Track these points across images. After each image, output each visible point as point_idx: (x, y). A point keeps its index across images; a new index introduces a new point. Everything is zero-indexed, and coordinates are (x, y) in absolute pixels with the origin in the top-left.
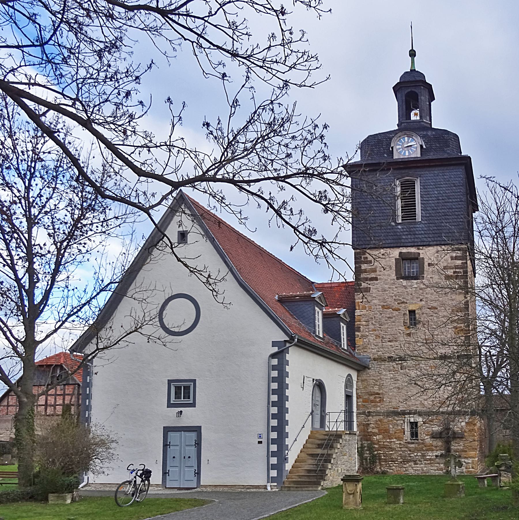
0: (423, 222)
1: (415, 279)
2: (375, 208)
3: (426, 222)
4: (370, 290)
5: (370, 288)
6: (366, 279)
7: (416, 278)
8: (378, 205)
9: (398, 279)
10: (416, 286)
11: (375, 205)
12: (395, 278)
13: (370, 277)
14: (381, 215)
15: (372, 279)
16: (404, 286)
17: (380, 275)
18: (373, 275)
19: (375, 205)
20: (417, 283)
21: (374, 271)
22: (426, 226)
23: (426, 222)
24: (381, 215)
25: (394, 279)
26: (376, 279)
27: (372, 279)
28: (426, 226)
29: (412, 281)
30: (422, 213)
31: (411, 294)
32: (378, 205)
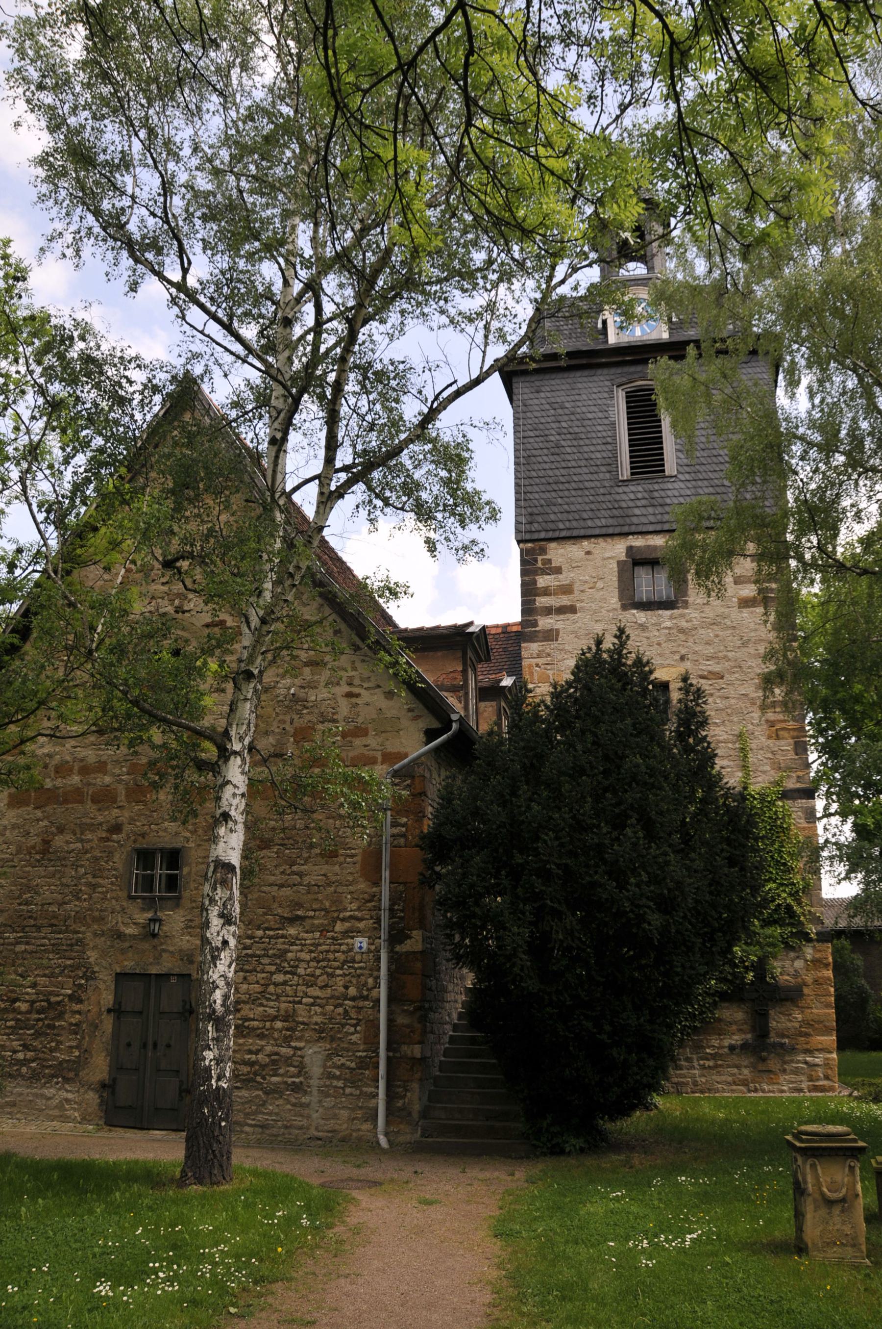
0: (680, 476)
1: (666, 609)
2: (568, 450)
3: (687, 477)
4: (558, 635)
5: (557, 631)
6: (548, 611)
7: (668, 605)
8: (575, 443)
9: (624, 607)
10: (668, 624)
11: (569, 443)
12: (619, 605)
13: (558, 605)
14: (583, 463)
15: (562, 610)
16: (641, 625)
17: (582, 601)
18: (564, 600)
19: (569, 443)
20: (671, 618)
21: (567, 590)
22: (689, 485)
23: (687, 477)
24: (583, 463)
25: (615, 609)
26: (572, 609)
27: (562, 610)
28: (689, 485)
29: (660, 612)
30: (678, 458)
31: (659, 644)
32: (575, 443)
